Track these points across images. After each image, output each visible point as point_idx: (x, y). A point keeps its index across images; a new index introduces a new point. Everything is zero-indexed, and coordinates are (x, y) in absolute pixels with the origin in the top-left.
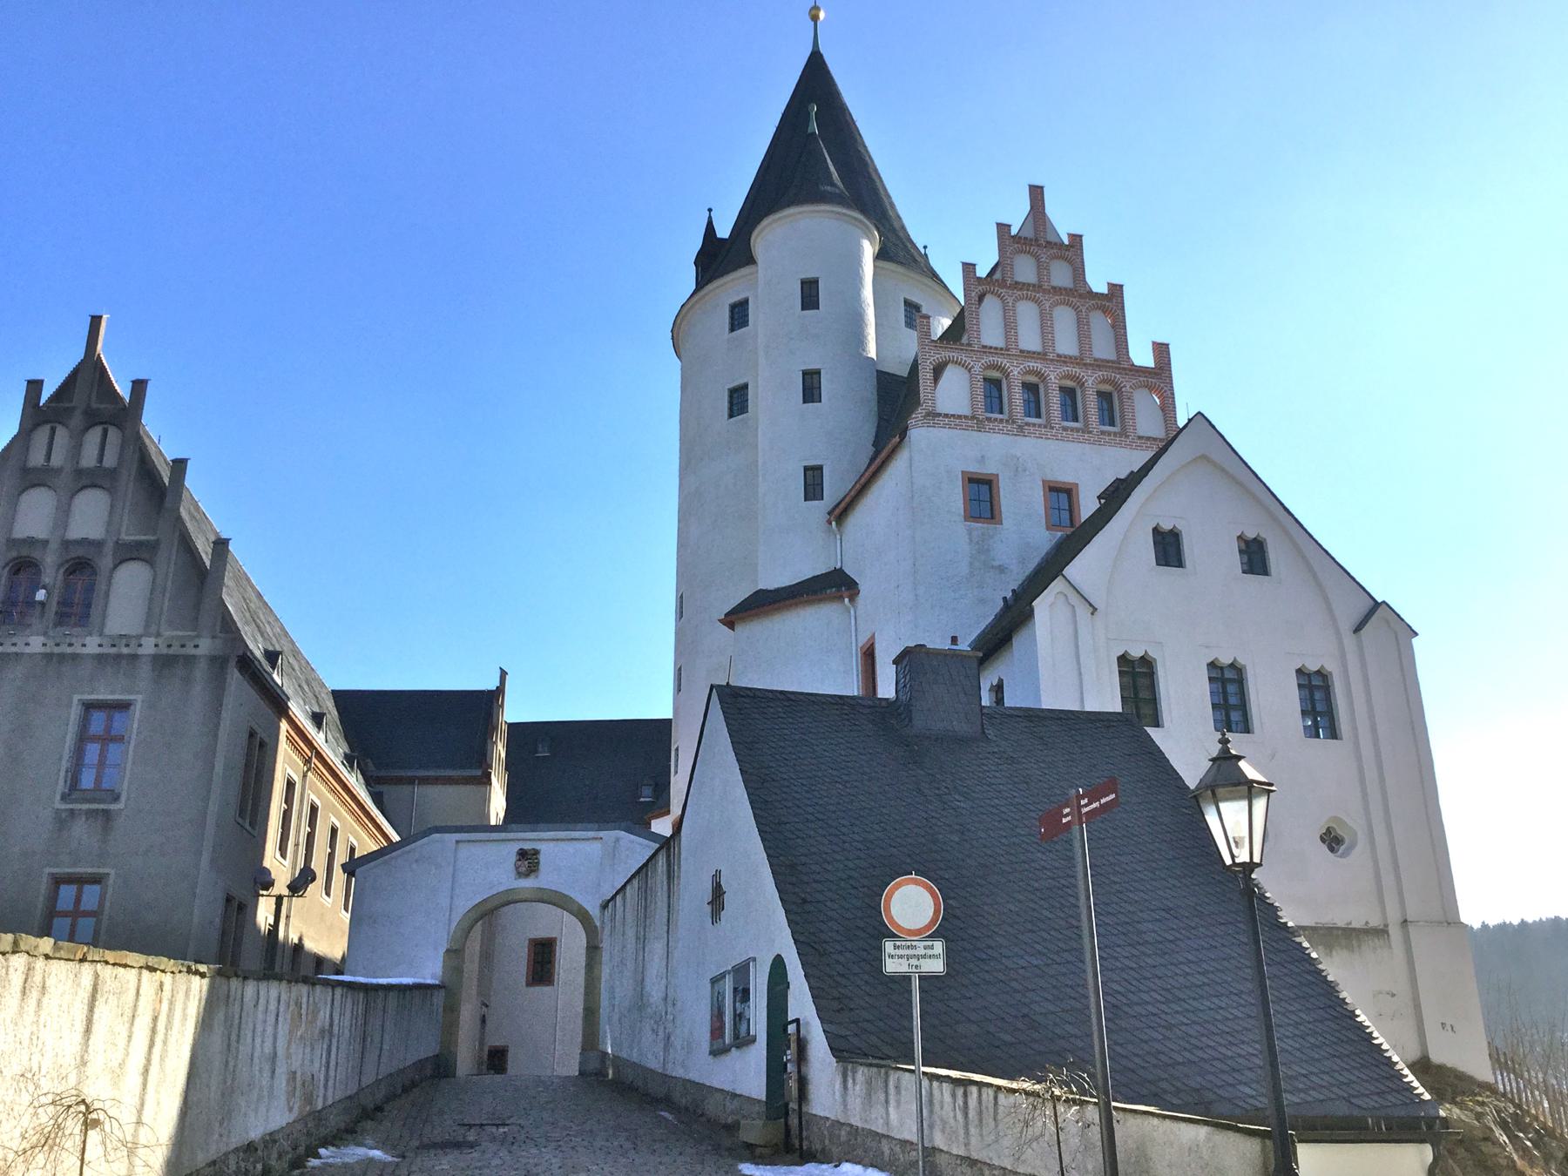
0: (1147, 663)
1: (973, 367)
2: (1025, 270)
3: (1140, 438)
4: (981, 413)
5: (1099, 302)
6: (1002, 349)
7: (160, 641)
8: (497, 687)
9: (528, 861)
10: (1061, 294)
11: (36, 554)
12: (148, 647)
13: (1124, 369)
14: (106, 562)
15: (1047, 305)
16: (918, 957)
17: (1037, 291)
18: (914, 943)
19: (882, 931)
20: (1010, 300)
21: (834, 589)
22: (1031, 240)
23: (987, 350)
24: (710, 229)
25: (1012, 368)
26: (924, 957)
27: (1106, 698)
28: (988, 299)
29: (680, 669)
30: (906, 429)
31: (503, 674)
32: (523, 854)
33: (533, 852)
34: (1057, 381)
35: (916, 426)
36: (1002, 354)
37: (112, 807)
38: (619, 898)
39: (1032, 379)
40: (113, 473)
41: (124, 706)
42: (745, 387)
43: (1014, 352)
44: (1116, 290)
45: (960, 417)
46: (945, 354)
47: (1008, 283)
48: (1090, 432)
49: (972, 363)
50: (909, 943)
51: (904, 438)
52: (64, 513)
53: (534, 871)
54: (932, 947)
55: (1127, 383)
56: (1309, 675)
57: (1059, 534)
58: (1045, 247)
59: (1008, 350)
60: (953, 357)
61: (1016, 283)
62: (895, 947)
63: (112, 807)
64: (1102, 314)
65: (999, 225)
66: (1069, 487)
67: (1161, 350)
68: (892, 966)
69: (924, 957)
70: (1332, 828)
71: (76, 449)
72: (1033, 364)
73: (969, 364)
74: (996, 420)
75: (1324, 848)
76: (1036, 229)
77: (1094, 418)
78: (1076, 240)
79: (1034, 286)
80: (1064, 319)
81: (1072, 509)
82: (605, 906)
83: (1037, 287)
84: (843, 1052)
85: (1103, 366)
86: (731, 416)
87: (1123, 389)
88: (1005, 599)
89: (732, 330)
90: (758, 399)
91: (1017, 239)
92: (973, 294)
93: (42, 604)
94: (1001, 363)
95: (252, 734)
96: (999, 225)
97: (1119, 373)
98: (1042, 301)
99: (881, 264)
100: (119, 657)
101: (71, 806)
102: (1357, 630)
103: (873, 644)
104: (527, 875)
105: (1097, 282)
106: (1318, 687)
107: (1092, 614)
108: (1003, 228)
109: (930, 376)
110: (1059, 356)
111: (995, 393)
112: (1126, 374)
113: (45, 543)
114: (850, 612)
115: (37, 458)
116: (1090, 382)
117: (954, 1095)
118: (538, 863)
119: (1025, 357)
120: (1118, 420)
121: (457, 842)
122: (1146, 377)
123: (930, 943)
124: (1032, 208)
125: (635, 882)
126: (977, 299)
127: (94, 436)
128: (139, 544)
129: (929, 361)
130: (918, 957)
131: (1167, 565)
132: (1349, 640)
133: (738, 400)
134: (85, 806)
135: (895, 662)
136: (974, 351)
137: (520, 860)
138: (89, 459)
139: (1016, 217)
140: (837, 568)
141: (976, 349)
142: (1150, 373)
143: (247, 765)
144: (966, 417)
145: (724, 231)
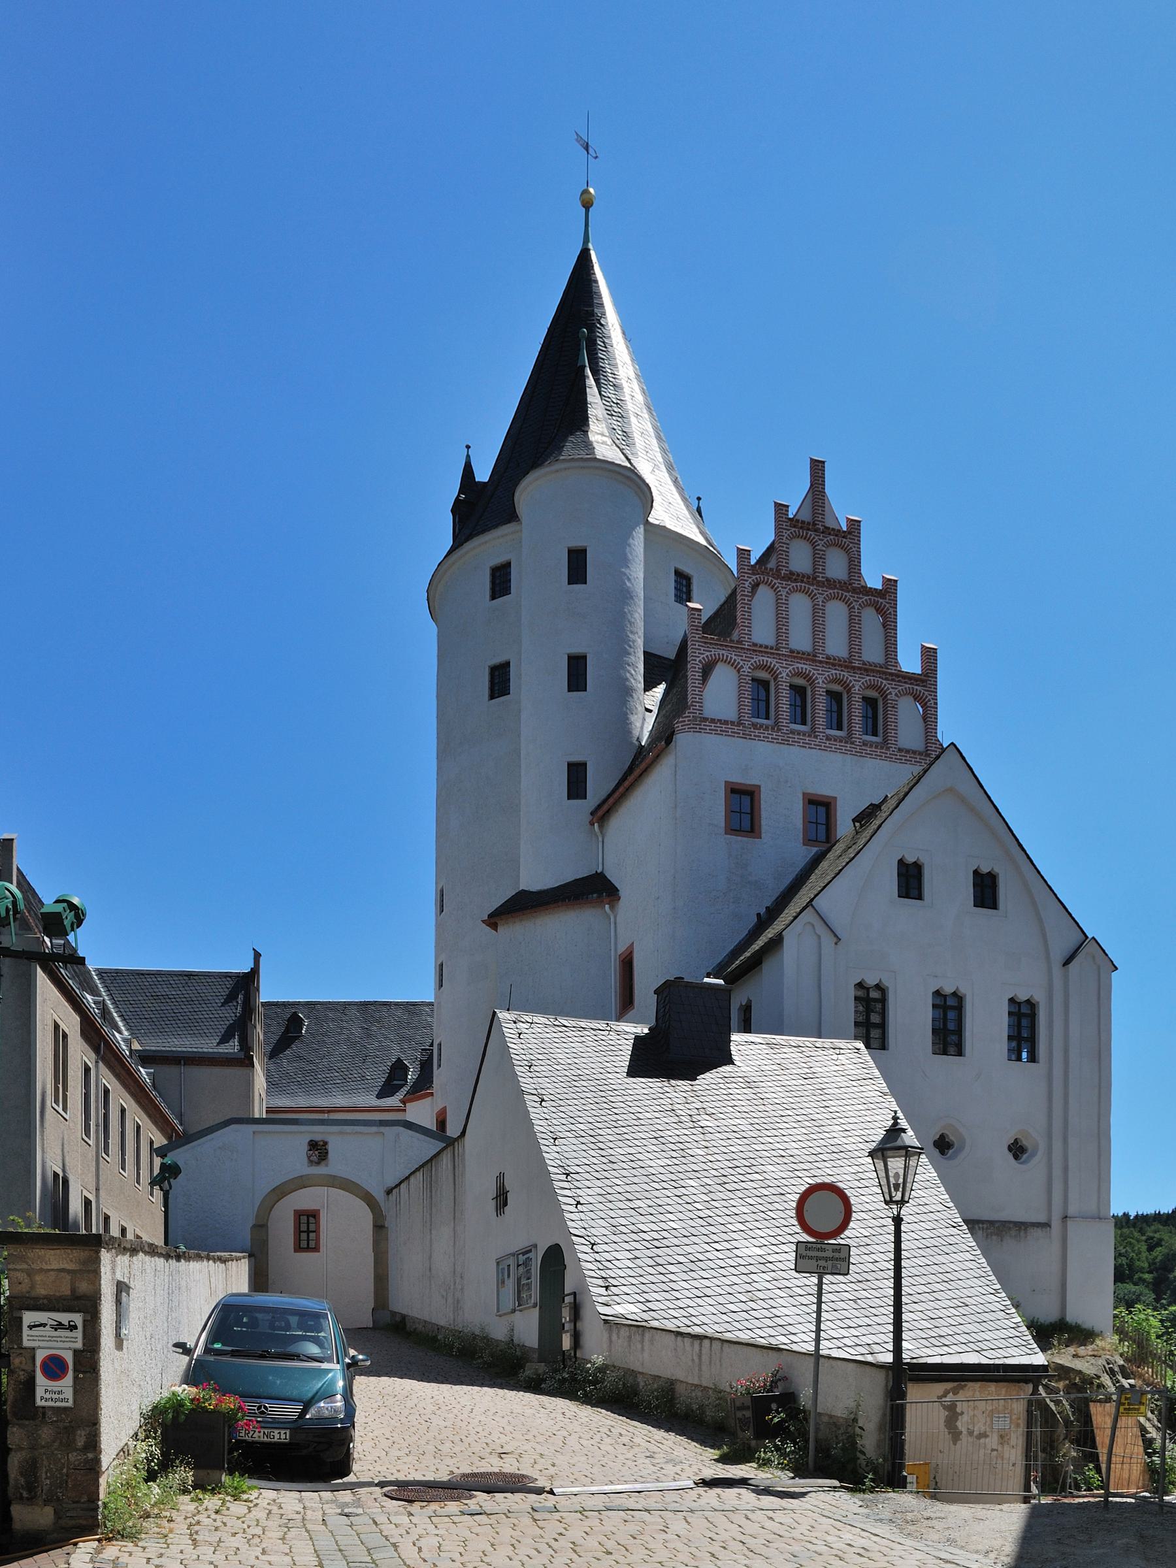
1: (742, 667)
2: (800, 558)
3: (900, 750)
4: (748, 720)
5: (873, 598)
9: (318, 1151)
10: (835, 587)
13: (891, 674)
15: (820, 600)
21: (595, 895)
22: (809, 523)
23: (757, 649)
25: (781, 669)
28: (762, 589)
30: (673, 733)
32: (313, 1145)
33: (321, 1143)
34: (825, 686)
35: (682, 731)
39: (800, 681)
45: (726, 722)
47: (783, 572)
48: (852, 743)
49: (741, 663)
57: (815, 850)
59: (777, 649)
61: (792, 573)
64: (875, 612)
67: (929, 656)
72: (805, 667)
73: (739, 663)
74: (761, 726)
76: (814, 513)
77: (857, 728)
78: (854, 525)
79: (809, 577)
80: (836, 613)
85: (873, 671)
87: (889, 697)
88: (759, 915)
91: (794, 522)
92: (747, 584)
94: (771, 663)
97: (886, 679)
103: (631, 953)
104: (318, 1163)
108: (780, 509)
109: (698, 676)
110: (828, 658)
111: (762, 693)
112: (893, 680)
116: (857, 688)
118: (327, 1153)
119: (795, 657)
122: (911, 684)
124: (812, 485)
125: (419, 1175)
126: (750, 590)
129: (698, 659)
136: (744, 648)
137: (310, 1150)
139: (795, 498)
144: (732, 723)
145: (483, 474)
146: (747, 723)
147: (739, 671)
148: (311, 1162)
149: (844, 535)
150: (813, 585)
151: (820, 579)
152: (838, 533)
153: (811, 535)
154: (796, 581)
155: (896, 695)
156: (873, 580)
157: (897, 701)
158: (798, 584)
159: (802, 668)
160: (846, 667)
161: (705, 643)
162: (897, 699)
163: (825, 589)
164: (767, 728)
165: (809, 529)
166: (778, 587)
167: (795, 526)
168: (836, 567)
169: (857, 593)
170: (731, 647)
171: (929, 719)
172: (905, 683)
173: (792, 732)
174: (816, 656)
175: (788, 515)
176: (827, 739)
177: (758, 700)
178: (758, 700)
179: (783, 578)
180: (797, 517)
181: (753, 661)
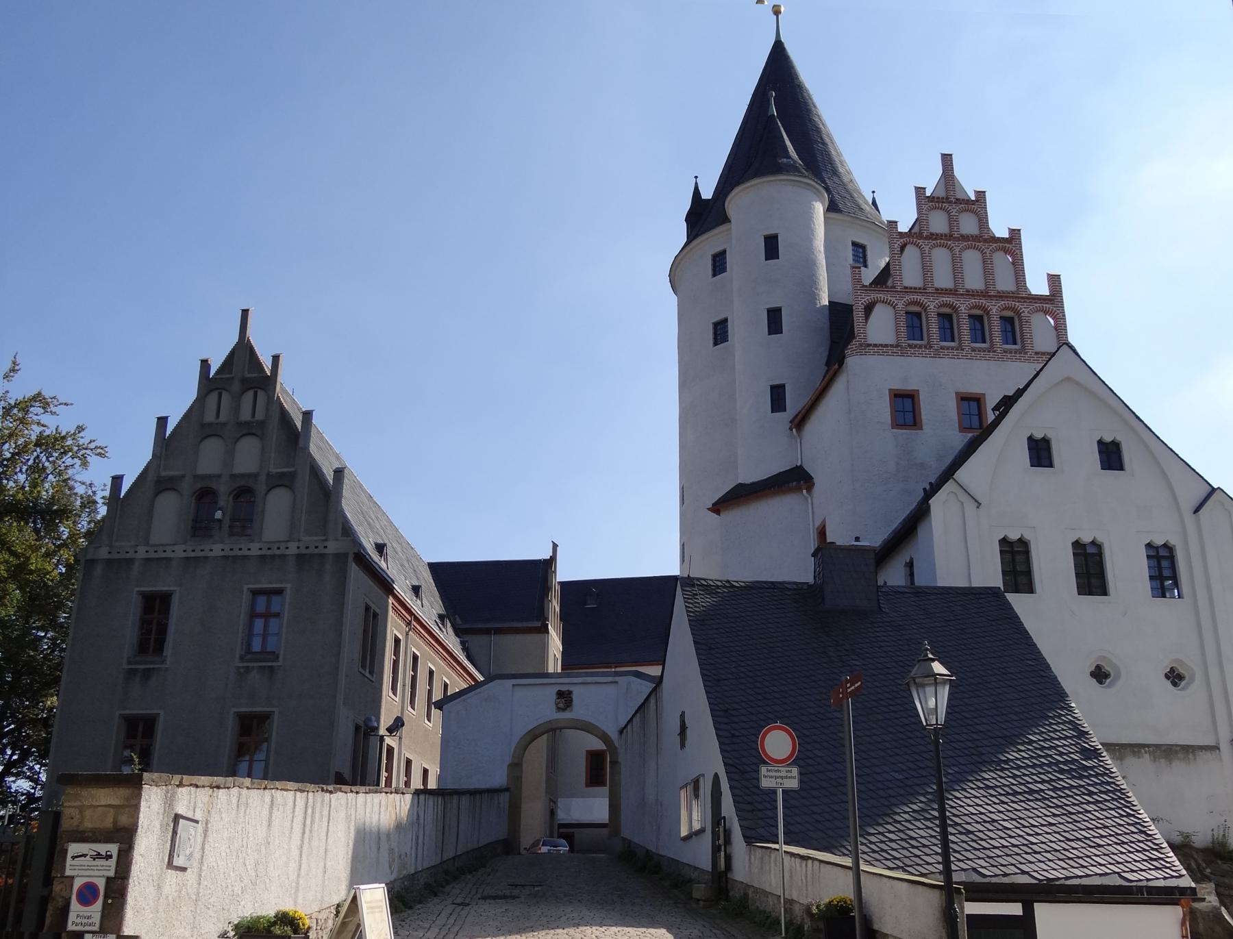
0: (1023, 543)
3: (1037, 353)
4: (904, 342)
6: (920, 289)
7: (301, 545)
8: (551, 557)
11: (214, 486)
12: (293, 549)
13: (1023, 298)
14: (261, 488)
16: (782, 778)
17: (948, 239)
18: (779, 768)
19: (761, 759)
20: (927, 249)
22: (943, 198)
23: (908, 290)
24: (697, 193)
25: (929, 303)
26: (786, 777)
27: (989, 574)
29: (683, 545)
30: (844, 357)
31: (555, 546)
32: (560, 694)
33: (567, 693)
34: (967, 312)
36: (920, 293)
37: (274, 664)
38: (629, 726)
40: (262, 424)
41: (279, 592)
42: (726, 320)
43: (930, 290)
44: (1015, 235)
45: (886, 346)
46: (874, 296)
47: (924, 234)
48: (994, 352)
50: (776, 768)
51: (842, 365)
52: (230, 454)
53: (568, 706)
54: (791, 771)
55: (1024, 309)
56: (1157, 548)
58: (955, 203)
59: (924, 289)
60: (880, 297)
61: (932, 234)
62: (768, 770)
63: (274, 664)
64: (1004, 253)
65: (917, 188)
66: (978, 397)
67: (1054, 281)
68: (766, 783)
69: (786, 777)
70: (1176, 668)
71: (237, 408)
72: (946, 299)
73: (894, 302)
74: (916, 346)
75: (1168, 683)
76: (947, 190)
77: (998, 339)
78: (981, 195)
79: (946, 235)
80: (972, 259)
81: (981, 414)
82: (621, 732)
83: (949, 237)
84: (749, 840)
85: (1007, 297)
86: (716, 344)
87: (1022, 314)
88: (925, 489)
89: (714, 275)
90: (735, 330)
91: (931, 199)
93: (219, 520)
94: (920, 299)
95: (367, 608)
96: (917, 188)
98: (953, 247)
99: (832, 215)
100: (273, 557)
101: (245, 664)
102: (1196, 511)
103: (824, 526)
104: (564, 710)
105: (1000, 230)
106: (1164, 557)
107: (978, 507)
108: (920, 191)
109: (861, 314)
110: (968, 291)
112: (1024, 302)
113: (219, 476)
114: (808, 501)
115: (210, 417)
116: (994, 310)
117: (801, 866)
118: (572, 700)
119: (940, 293)
120: (1019, 340)
121: (513, 685)
122: (1041, 303)
123: (790, 769)
126: (899, 249)
127: (249, 395)
128: (283, 475)
130: (782, 778)
131: (1039, 465)
132: (1189, 517)
133: (720, 332)
134: (256, 664)
135: (814, 555)
137: (558, 698)
138: (245, 415)
140: (798, 465)
141: (899, 290)
142: (1045, 300)
143: (365, 631)
144: (892, 346)
146: (904, 344)
147: (894, 307)
148: (559, 709)
149: (973, 202)
150: (950, 240)
151: (956, 236)
152: (968, 201)
153: (945, 206)
154: (936, 239)
155: (1028, 312)
156: (1000, 231)
157: (1029, 317)
158: (938, 241)
159: (946, 301)
160: (984, 296)
161: (866, 290)
162: (1029, 315)
163: (960, 242)
164: (921, 347)
165: (943, 202)
166: (922, 245)
167: (932, 202)
168: (968, 225)
169: (987, 243)
170: (887, 291)
171: (1060, 328)
172: (1036, 303)
173: (942, 348)
174: (957, 291)
175: (925, 194)
176: (972, 351)
177: (913, 327)
178: (913, 327)
179: (926, 238)
180: (933, 195)
181: (905, 299)
